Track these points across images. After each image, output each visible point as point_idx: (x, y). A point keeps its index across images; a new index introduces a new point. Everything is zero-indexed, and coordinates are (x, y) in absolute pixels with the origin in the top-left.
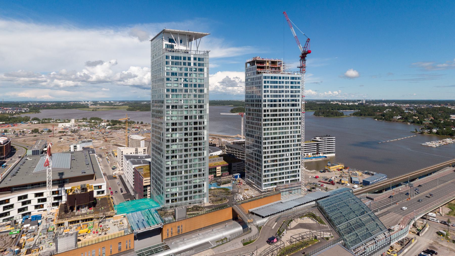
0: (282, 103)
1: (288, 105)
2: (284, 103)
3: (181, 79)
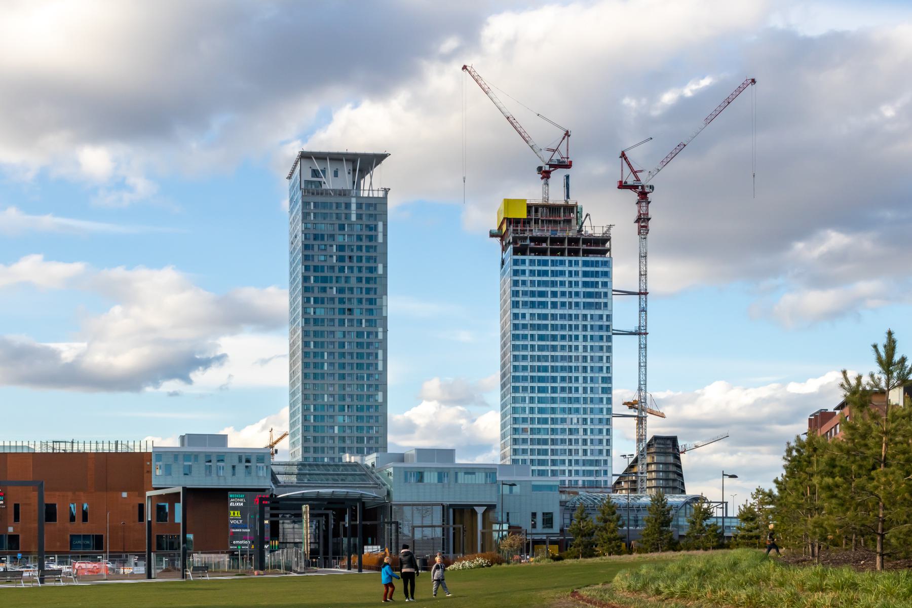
0: (559, 300)
1: (577, 304)
2: (566, 299)
3: (331, 246)
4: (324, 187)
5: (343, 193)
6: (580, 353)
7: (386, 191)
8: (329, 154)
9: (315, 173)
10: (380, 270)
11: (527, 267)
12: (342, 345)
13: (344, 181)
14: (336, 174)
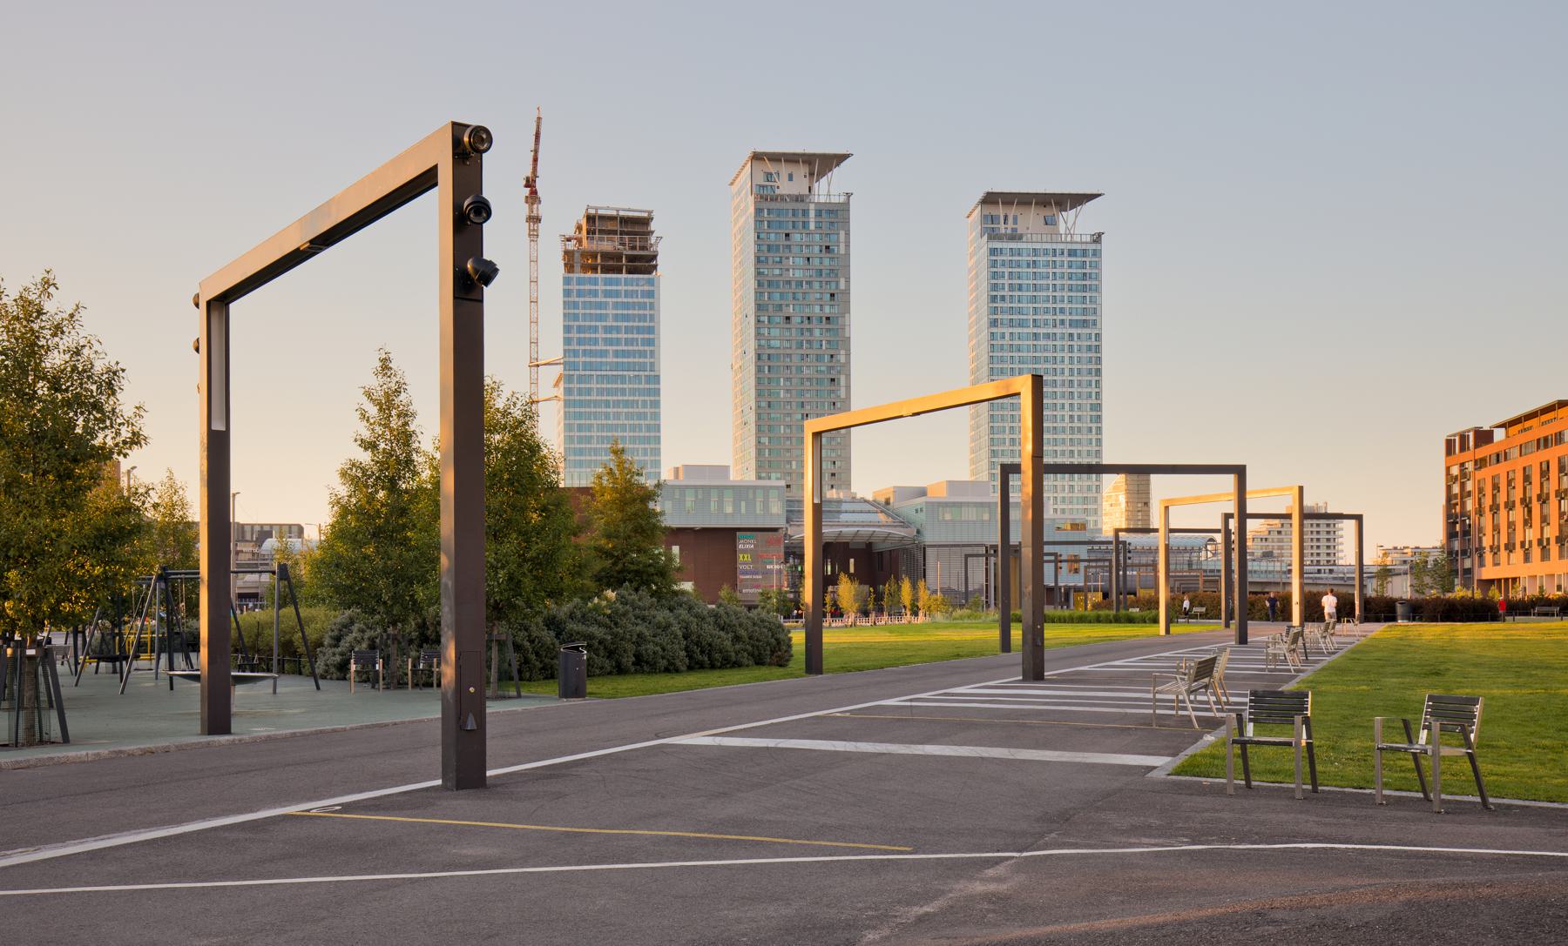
1: (1062, 322)
4: (778, 192)
5: (799, 199)
6: (1067, 377)
7: (848, 195)
8: (784, 154)
9: (769, 176)
10: (842, 286)
11: (1006, 282)
12: (800, 369)
13: (798, 186)
14: (791, 177)
